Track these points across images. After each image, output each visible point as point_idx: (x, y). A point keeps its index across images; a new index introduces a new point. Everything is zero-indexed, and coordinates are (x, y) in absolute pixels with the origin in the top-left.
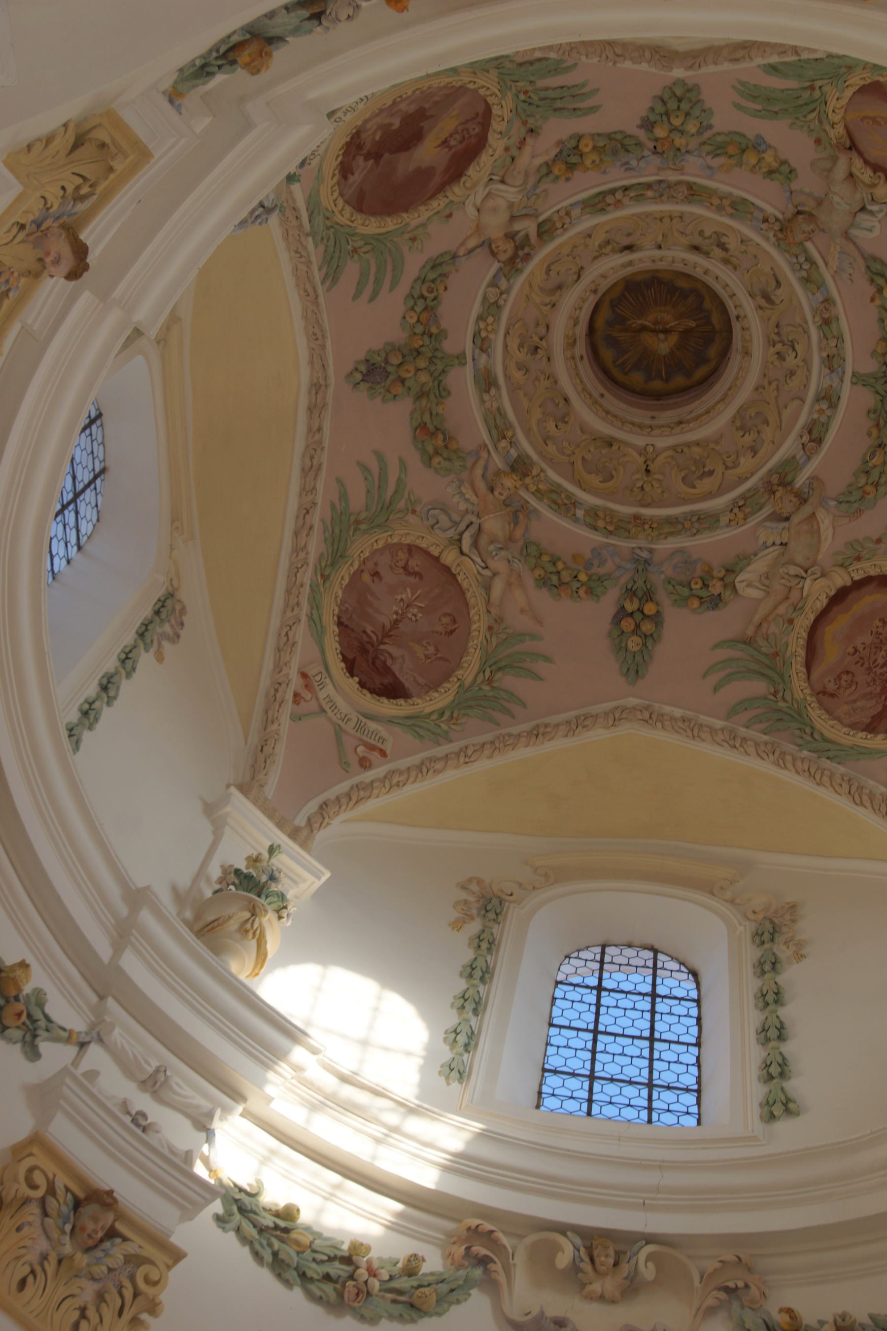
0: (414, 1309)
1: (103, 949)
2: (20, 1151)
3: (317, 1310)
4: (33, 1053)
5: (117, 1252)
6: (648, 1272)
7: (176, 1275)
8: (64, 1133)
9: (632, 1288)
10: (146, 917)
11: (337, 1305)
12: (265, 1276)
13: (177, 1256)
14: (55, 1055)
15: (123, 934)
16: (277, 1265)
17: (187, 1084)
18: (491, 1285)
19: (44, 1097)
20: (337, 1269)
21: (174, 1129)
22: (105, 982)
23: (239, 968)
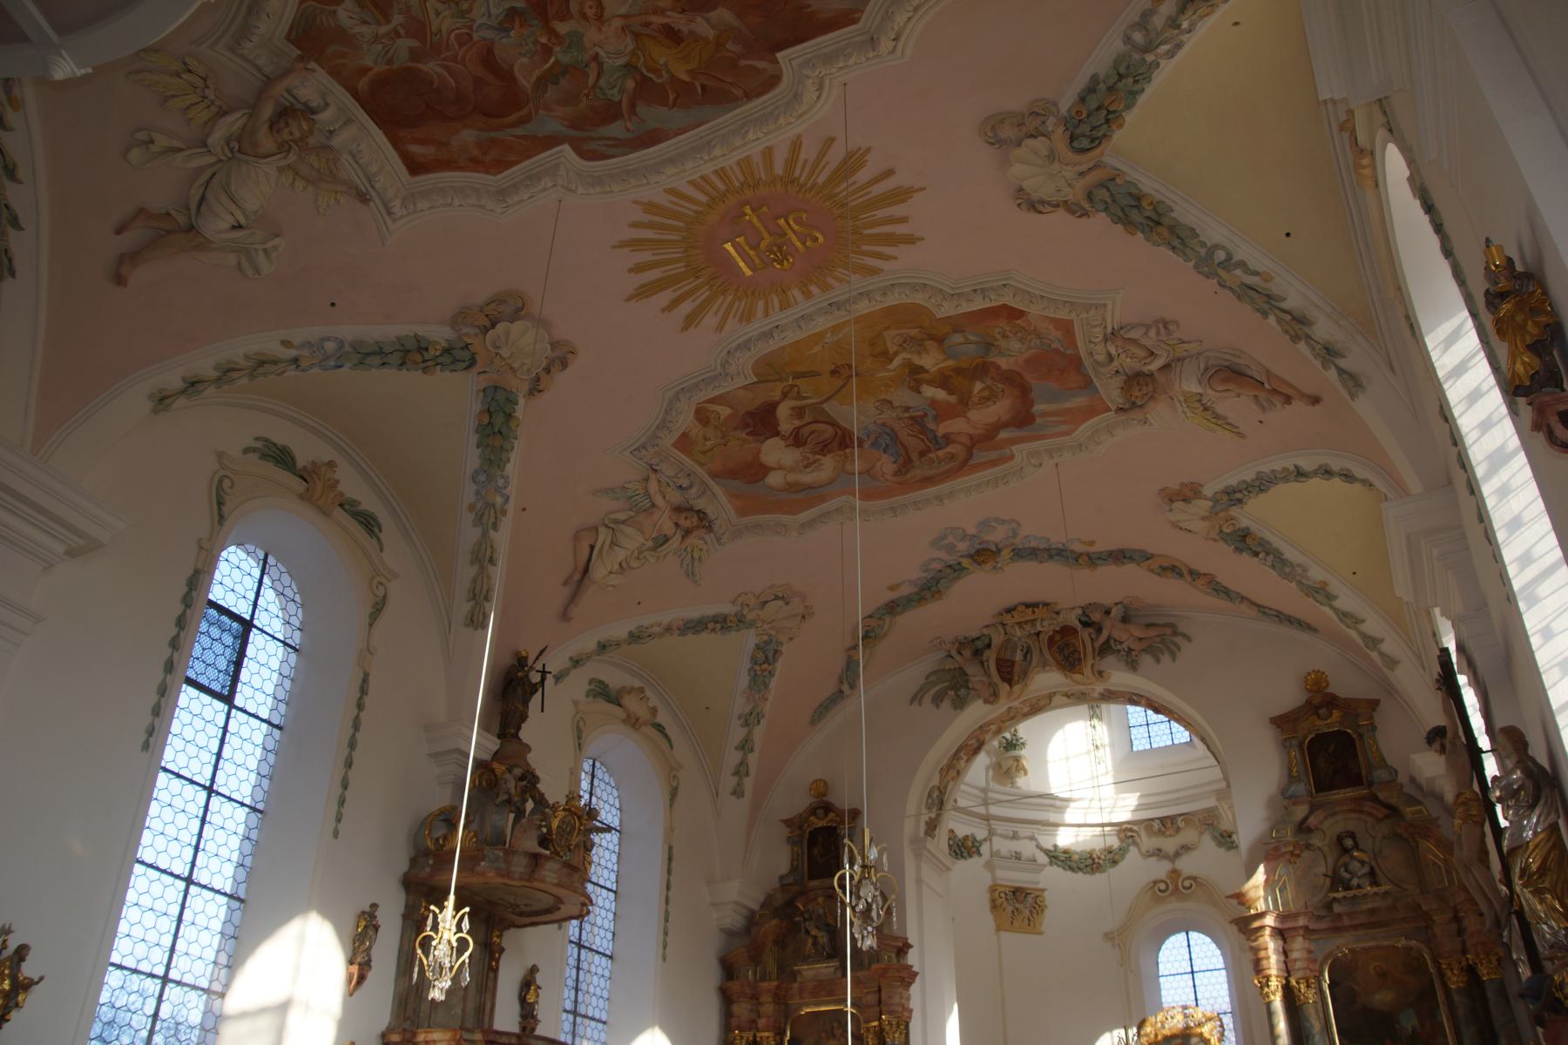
0: (1115, 862)
1: (982, 810)
2: (993, 889)
3: (1087, 876)
4: (980, 854)
5: (1030, 899)
6: (1181, 824)
7: (1046, 894)
8: (1000, 874)
9: (1178, 830)
10: (990, 795)
11: (1093, 871)
12: (1069, 873)
13: (1043, 890)
14: (985, 849)
15: (986, 803)
16: (1071, 869)
17: (1024, 831)
18: (1135, 844)
19: (989, 866)
20: (1089, 862)
21: (1027, 848)
22: (987, 818)
23: (1022, 782)
